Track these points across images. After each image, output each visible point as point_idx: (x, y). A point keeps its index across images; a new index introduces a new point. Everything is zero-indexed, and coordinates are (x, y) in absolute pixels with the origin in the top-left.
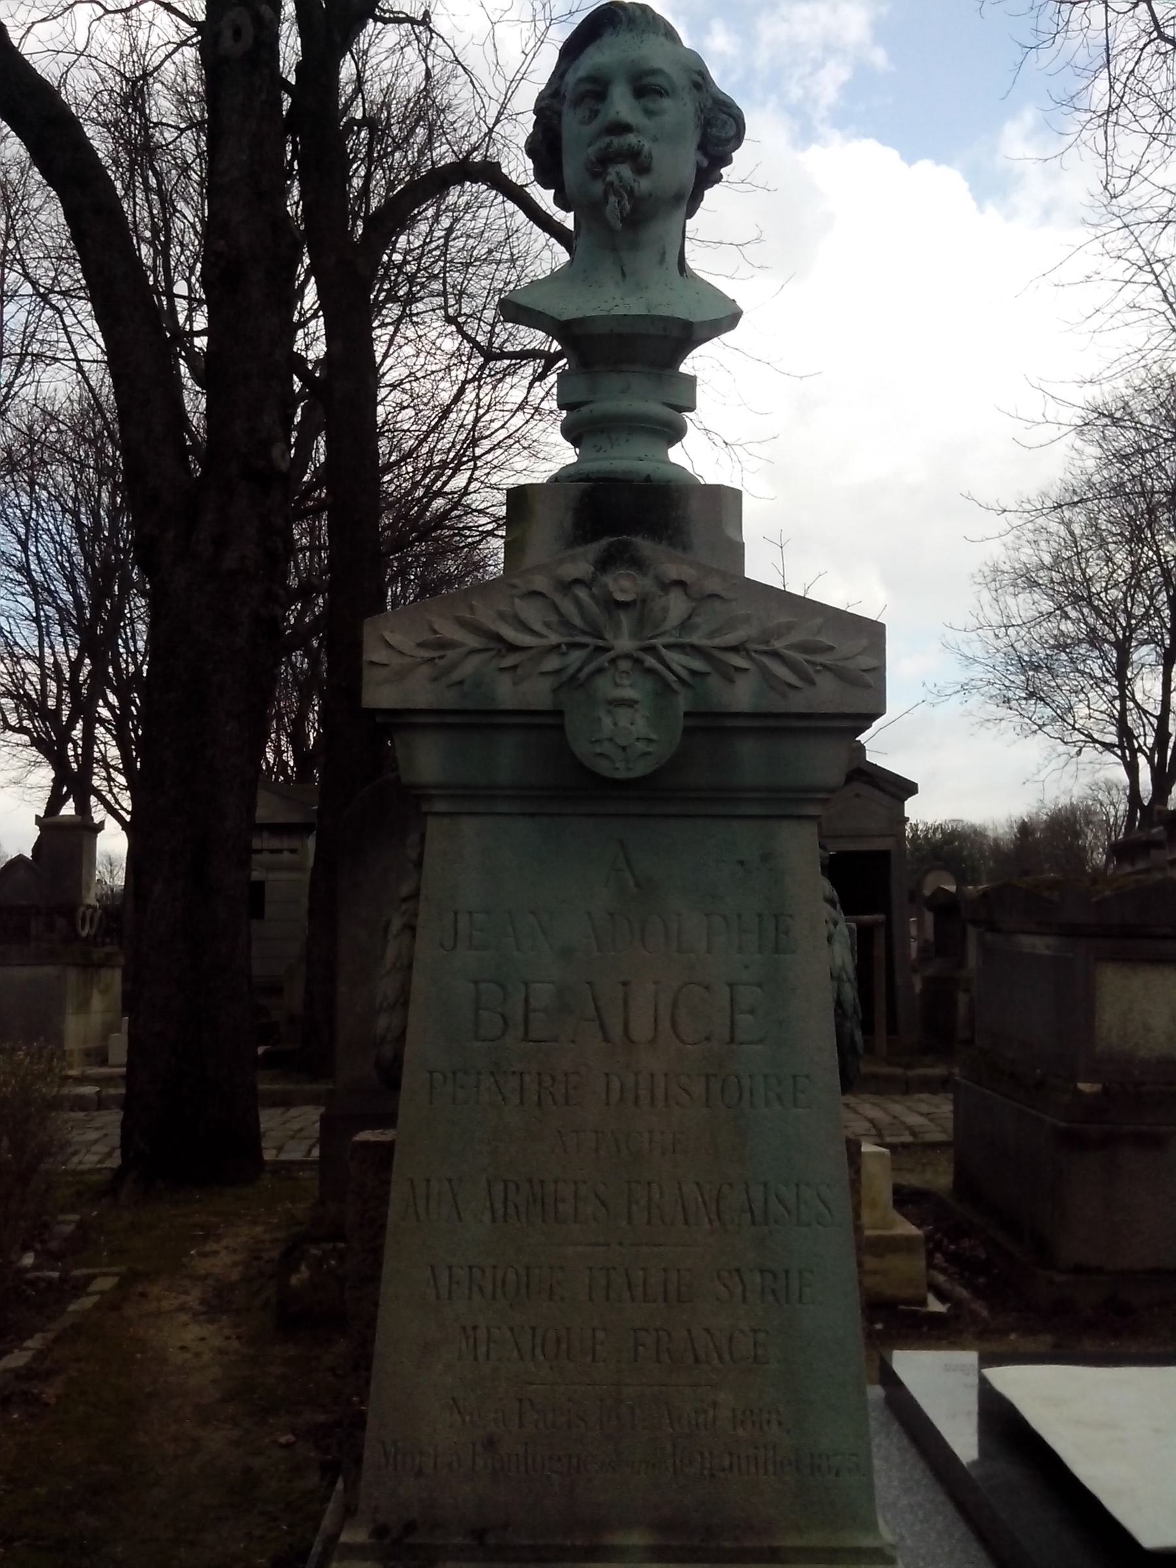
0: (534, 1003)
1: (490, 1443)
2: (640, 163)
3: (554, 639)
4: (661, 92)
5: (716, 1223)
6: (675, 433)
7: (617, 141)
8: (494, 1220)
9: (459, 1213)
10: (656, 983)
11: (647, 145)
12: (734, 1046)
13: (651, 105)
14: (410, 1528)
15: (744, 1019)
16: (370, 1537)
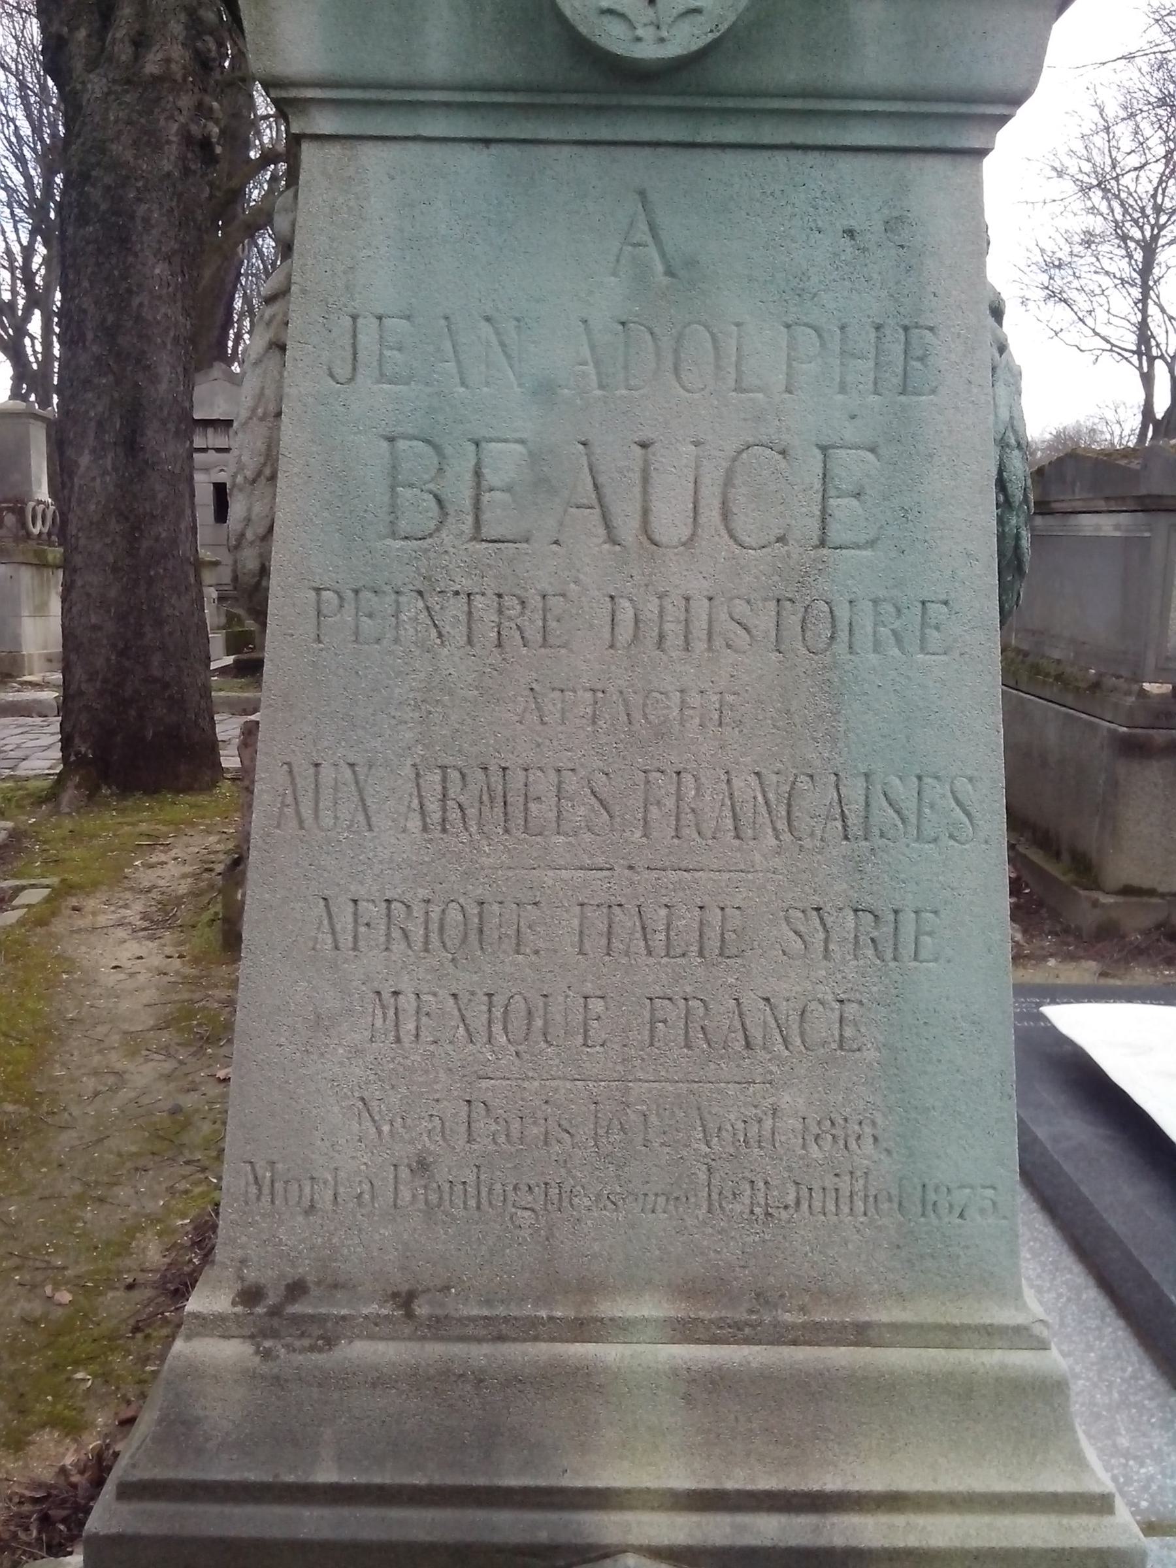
0: (491, 477)
1: (422, 1166)
5: (786, 837)
8: (425, 829)
9: (368, 818)
10: (697, 444)
12: (825, 551)
14: (297, 1289)
16: (234, 1304)
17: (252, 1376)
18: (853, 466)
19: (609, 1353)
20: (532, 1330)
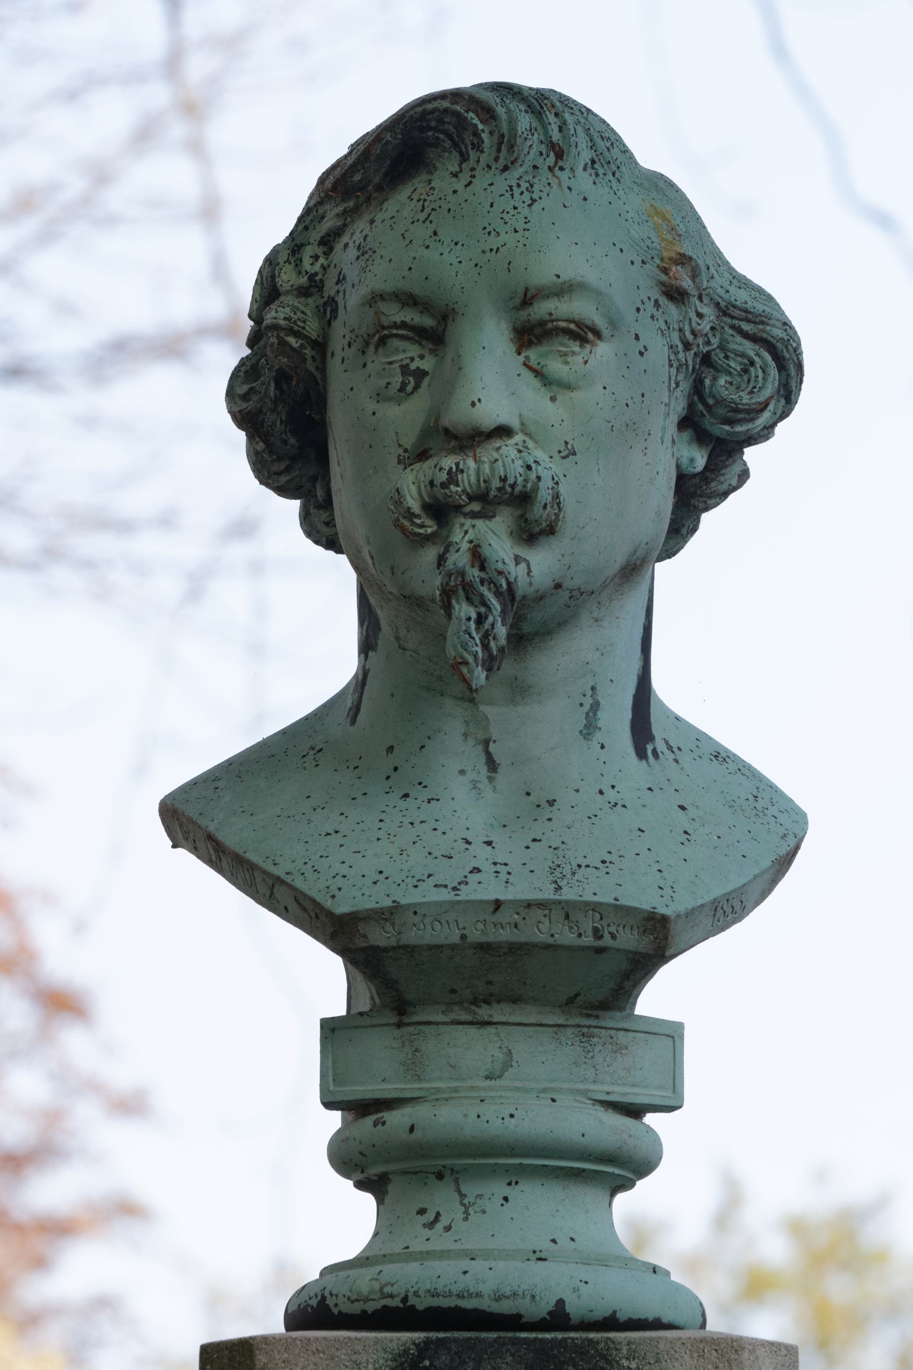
2: (529, 513)
4: (583, 333)
6: (627, 1166)
7: (473, 469)
11: (548, 467)
13: (555, 367)
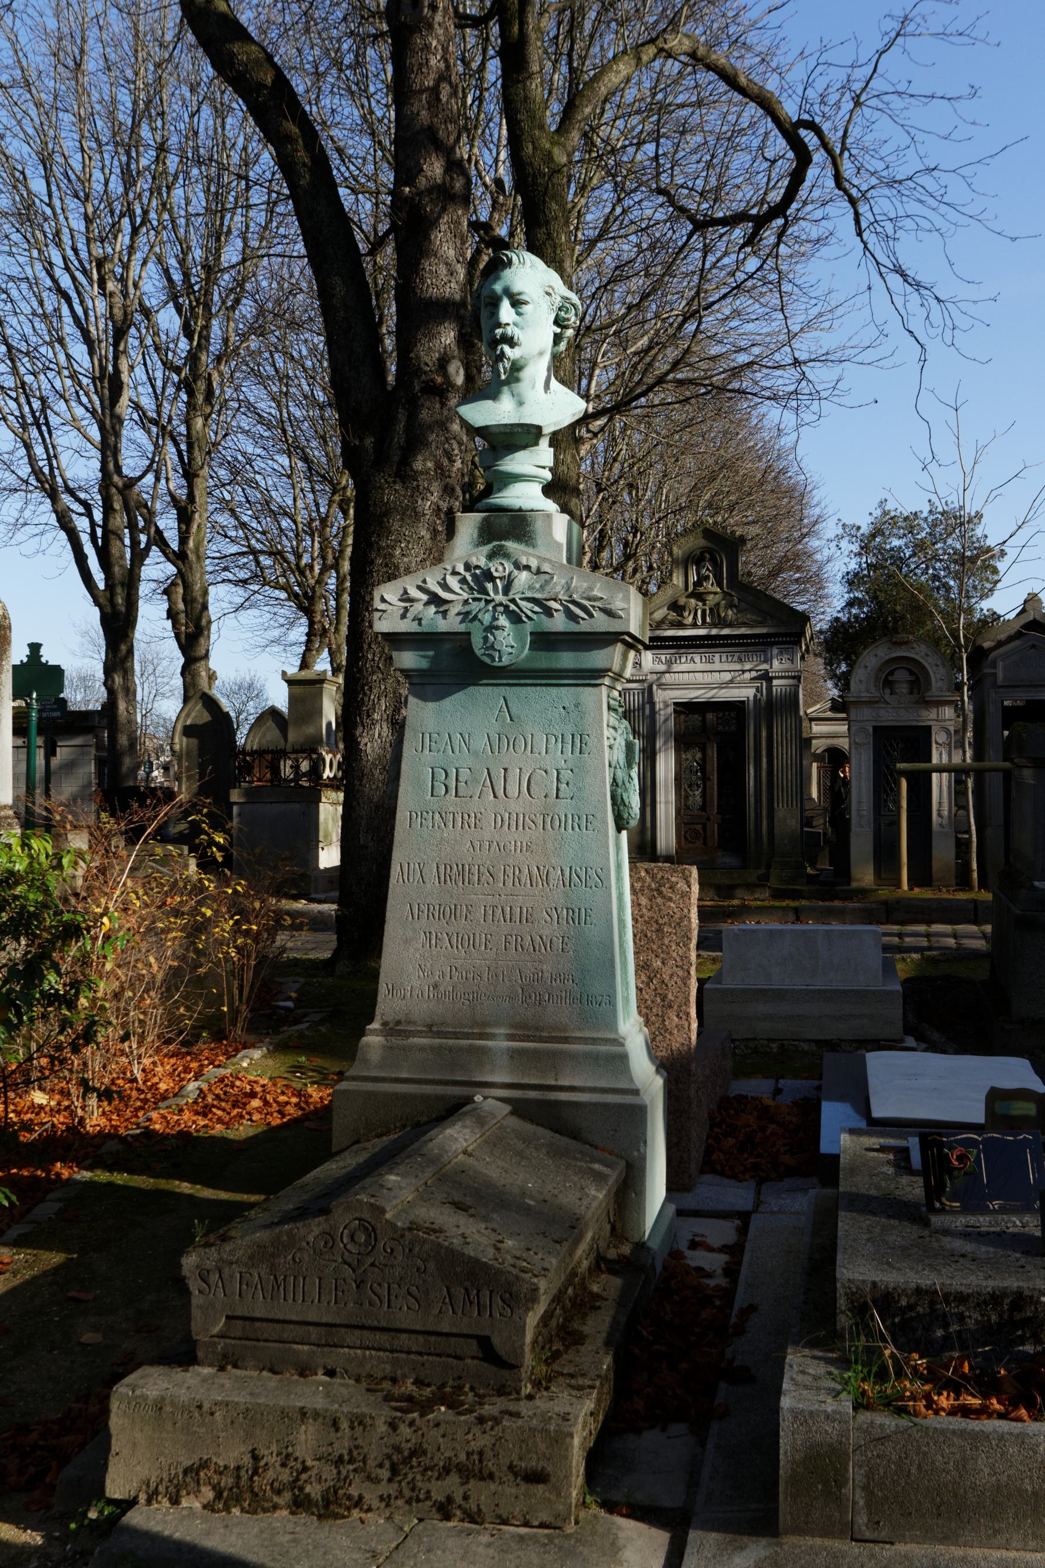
1: (436, 986)
3: (465, 596)
14: (398, 1023)
15: (563, 786)
17: (384, 1046)
18: (566, 775)
19: (490, 1043)
20: (467, 1036)
